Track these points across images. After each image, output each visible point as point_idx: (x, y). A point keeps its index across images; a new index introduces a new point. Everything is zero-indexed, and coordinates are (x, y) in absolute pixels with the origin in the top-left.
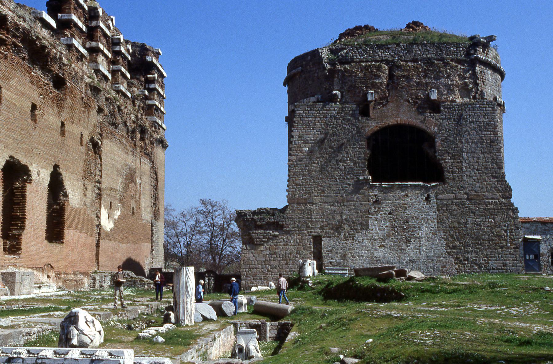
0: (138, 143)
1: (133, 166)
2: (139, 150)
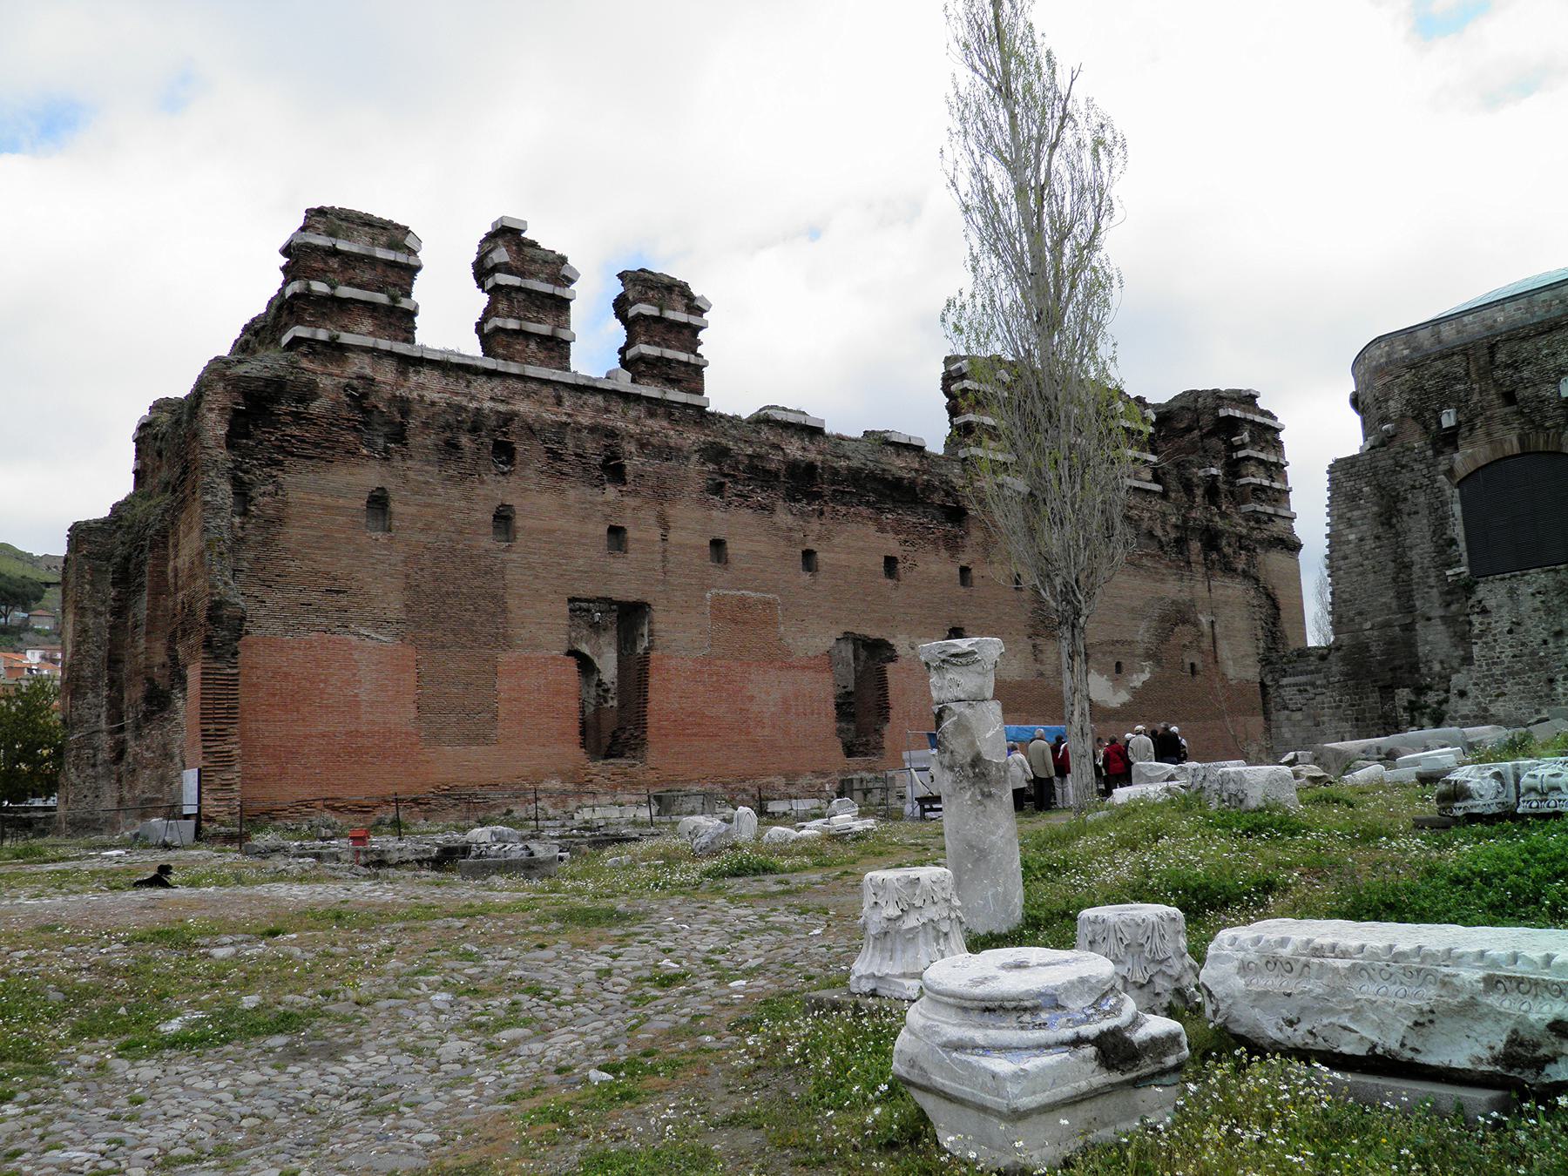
0: (1193, 558)
1: (1185, 596)
2: (1199, 570)
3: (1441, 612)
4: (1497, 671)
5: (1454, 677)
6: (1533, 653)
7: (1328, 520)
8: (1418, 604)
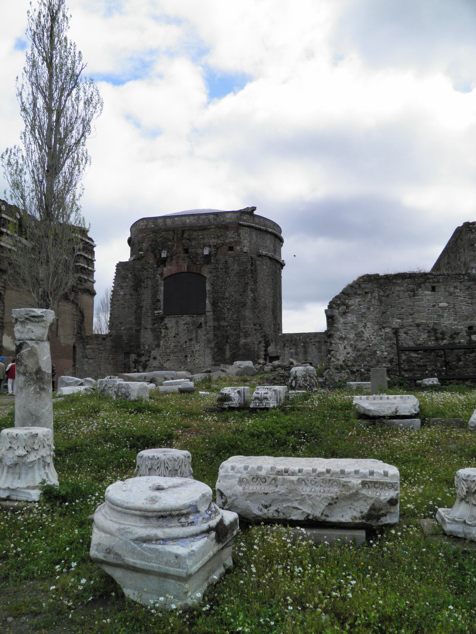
3: (151, 326)
4: (168, 351)
5: (152, 352)
6: (181, 346)
7: (113, 285)
8: (143, 322)
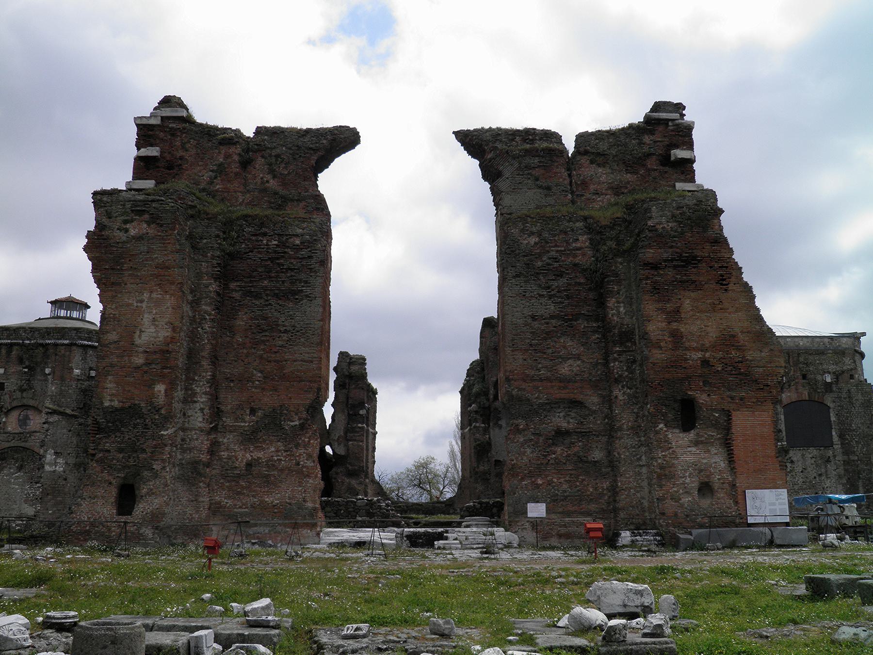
4: (796, 487)
6: (811, 482)
